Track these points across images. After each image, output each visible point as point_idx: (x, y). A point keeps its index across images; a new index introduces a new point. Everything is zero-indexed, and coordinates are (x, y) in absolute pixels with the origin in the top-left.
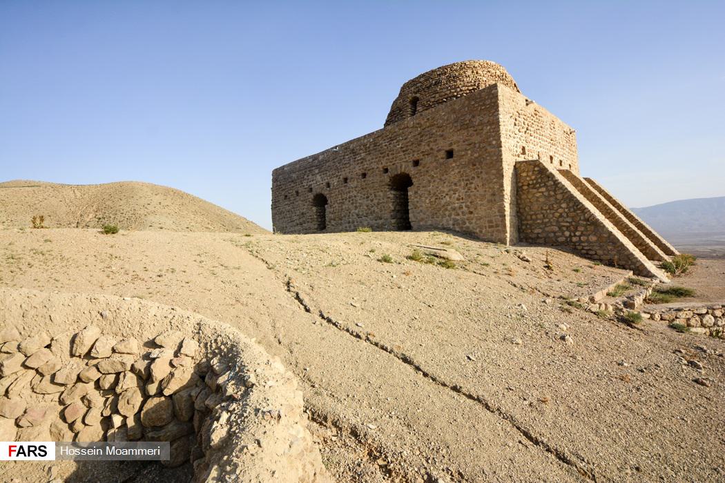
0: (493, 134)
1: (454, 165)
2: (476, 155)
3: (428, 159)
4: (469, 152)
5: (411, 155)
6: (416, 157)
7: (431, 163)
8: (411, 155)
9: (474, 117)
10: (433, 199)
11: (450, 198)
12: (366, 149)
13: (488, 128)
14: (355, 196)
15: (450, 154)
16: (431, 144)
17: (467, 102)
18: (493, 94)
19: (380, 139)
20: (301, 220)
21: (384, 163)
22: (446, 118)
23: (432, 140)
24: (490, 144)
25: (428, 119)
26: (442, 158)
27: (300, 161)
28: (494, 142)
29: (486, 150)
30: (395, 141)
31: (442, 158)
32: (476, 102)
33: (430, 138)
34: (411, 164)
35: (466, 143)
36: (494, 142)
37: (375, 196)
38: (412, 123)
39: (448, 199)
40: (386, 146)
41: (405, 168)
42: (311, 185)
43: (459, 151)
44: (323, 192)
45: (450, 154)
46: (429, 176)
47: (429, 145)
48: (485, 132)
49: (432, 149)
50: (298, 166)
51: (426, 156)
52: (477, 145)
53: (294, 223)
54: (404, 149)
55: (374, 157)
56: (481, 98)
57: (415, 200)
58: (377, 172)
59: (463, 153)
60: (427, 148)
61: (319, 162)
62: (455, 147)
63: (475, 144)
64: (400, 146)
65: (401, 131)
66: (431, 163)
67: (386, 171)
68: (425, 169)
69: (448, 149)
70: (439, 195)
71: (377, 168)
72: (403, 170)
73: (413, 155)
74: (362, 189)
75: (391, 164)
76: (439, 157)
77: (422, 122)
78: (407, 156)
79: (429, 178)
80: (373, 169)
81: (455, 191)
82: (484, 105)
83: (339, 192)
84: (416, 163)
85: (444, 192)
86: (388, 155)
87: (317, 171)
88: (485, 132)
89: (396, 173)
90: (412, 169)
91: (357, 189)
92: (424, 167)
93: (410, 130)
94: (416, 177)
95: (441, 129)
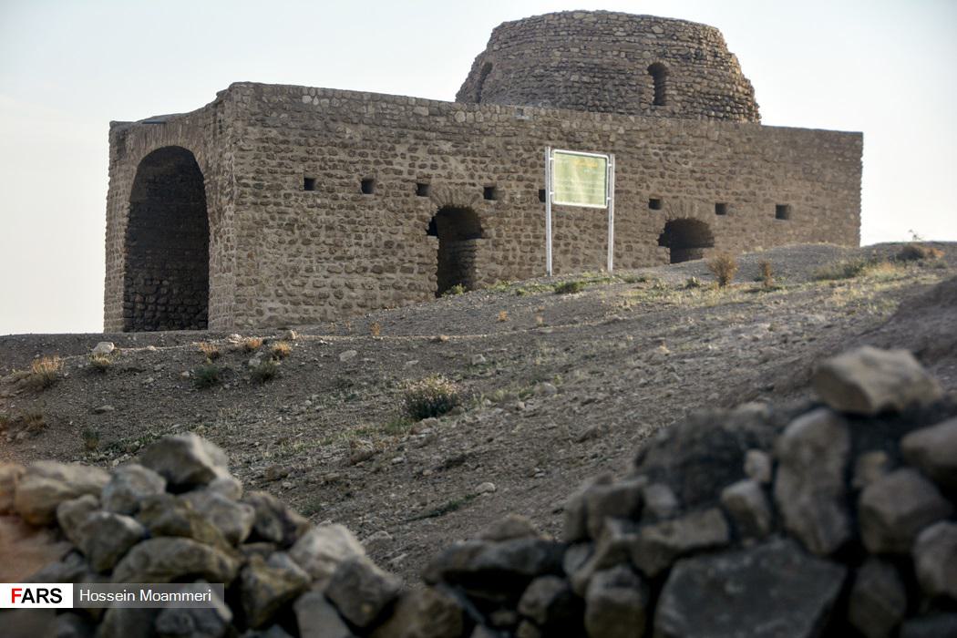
0: (852, 204)
1: (791, 232)
2: (826, 227)
3: (746, 209)
4: (816, 219)
5: (712, 191)
6: (723, 197)
7: (752, 217)
8: (712, 191)
9: (824, 166)
12: (605, 144)
13: (846, 192)
14: (575, 239)
15: (781, 212)
16: (752, 186)
17: (817, 141)
18: (856, 146)
19: (642, 135)
20: (380, 261)
21: (653, 188)
22: (779, 149)
23: (753, 177)
24: (846, 217)
25: (749, 140)
26: (769, 215)
27: (376, 98)
28: (852, 217)
29: (840, 224)
30: (678, 153)
31: (769, 215)
32: (831, 147)
33: (750, 173)
34: (713, 210)
35: (810, 203)
36: (852, 217)
37: (629, 248)
38: (717, 133)
40: (656, 154)
41: (700, 212)
42: (429, 177)
43: (799, 212)
44: (474, 206)
45: (781, 212)
46: (747, 238)
47: (747, 186)
48: (840, 196)
49: (754, 194)
50: (371, 110)
52: (828, 213)
53: (353, 265)
54: (698, 175)
55: (629, 169)
56: (838, 142)
58: (638, 202)
59: (807, 218)
60: (744, 189)
61: (455, 124)
62: (792, 203)
63: (824, 209)
64: (690, 166)
65: (691, 140)
66: (752, 217)
67: (654, 204)
68: (740, 225)
69: (782, 203)
71: (638, 193)
72: (695, 214)
73: (718, 193)
74: (595, 226)
75: (670, 195)
76: (766, 211)
77: (737, 140)
80: (628, 192)
82: (842, 155)
83: (527, 216)
86: (662, 175)
87: (447, 147)
88: (840, 196)
89: (681, 216)
90: (716, 217)
91: (583, 224)
92: (737, 221)
93: (711, 145)
94: (723, 235)
95: (769, 165)
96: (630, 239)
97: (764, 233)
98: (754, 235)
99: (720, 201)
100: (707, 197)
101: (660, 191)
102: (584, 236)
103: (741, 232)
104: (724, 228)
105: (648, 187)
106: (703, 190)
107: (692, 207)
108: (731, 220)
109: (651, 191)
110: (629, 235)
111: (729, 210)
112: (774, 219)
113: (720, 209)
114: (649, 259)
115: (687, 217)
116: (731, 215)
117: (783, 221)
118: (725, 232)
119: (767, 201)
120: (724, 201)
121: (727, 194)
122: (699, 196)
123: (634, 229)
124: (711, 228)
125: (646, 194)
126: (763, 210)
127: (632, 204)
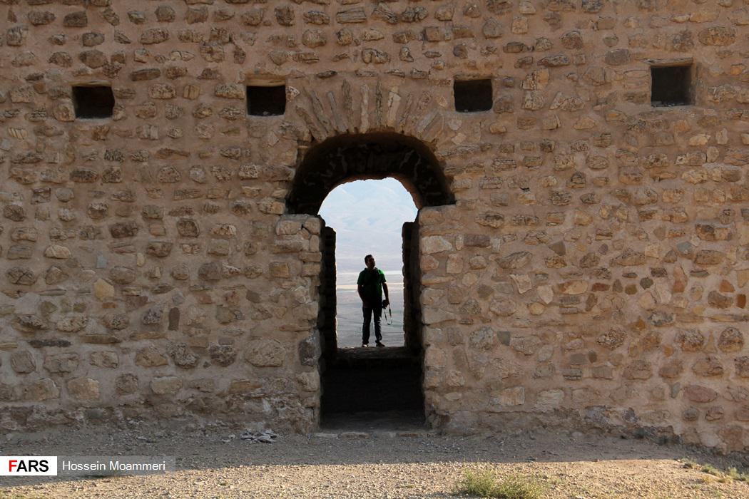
5: (444, 48)
6: (476, 63)
10: (580, 288)
11: (677, 289)
21: (257, 59)
26: (630, 97)
31: (630, 97)
34: (446, 98)
39: (666, 297)
41: (406, 109)
46: (557, 171)
51: (544, 73)
57: (470, 279)
58: (206, 100)
66: (573, 109)
68: (533, 134)
70: (617, 273)
71: (207, 75)
72: (391, 119)
73: (459, 52)
74: (78, 176)
75: (310, 71)
78: (414, 47)
79: (560, 185)
80: (176, 74)
81: (702, 263)
84: (473, 95)
85: (641, 259)
90: (457, 120)
92: (522, 124)
96: (189, 203)
97: (613, 149)
98: (579, 158)
99: (468, 74)
100: (422, 65)
101: (279, 63)
102: (45, 207)
103: (538, 153)
104: (483, 149)
105: (239, 56)
106: (414, 47)
107: (379, 98)
108: (501, 124)
109: (250, 66)
110: (185, 193)
111: (499, 95)
112: (647, 106)
113: (473, 95)
114: (250, 254)
115: (364, 129)
116: (507, 107)
117: (678, 110)
118: (487, 160)
119: (617, 59)
120: (484, 73)
121: (490, 51)
122: (399, 67)
123: (199, 173)
124: (440, 153)
125: (235, 78)
126: (605, 84)
127: (189, 106)
